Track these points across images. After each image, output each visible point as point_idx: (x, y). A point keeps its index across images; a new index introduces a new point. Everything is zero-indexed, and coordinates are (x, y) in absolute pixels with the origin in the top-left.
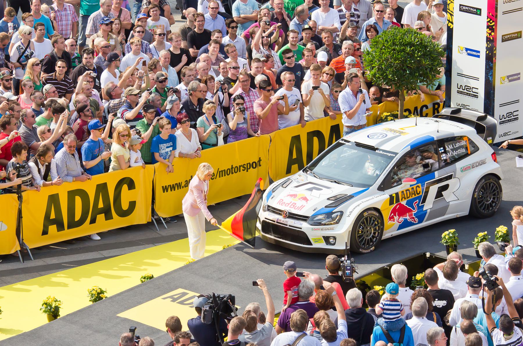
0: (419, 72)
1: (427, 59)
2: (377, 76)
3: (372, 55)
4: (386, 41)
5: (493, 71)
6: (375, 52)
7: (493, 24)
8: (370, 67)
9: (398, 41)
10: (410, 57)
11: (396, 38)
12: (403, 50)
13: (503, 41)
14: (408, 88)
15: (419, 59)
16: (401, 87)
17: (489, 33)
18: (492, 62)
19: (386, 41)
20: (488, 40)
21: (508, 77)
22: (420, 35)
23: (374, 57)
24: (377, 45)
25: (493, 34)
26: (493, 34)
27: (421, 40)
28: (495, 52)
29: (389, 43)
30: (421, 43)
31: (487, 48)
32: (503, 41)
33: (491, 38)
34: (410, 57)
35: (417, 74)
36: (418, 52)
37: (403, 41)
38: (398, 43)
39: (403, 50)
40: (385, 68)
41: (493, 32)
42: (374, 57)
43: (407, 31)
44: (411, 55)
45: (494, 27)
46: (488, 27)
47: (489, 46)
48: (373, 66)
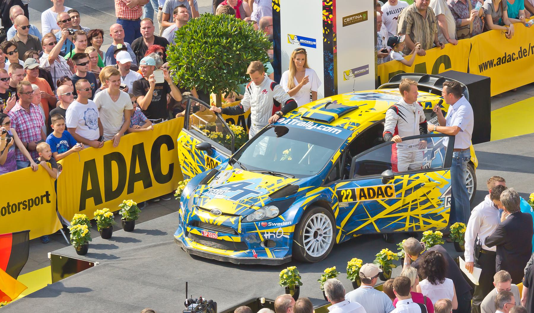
0: (239, 69)
1: (249, 53)
2: (186, 77)
3: (177, 52)
4: (196, 32)
5: (334, 64)
6: (182, 47)
7: (331, 3)
8: (176, 66)
9: (210, 31)
10: (228, 52)
11: (207, 27)
12: (218, 43)
13: (344, 25)
14: (226, 91)
15: (238, 52)
16: (218, 91)
17: (326, 16)
18: (332, 52)
19: (196, 32)
20: (325, 24)
21: (353, 71)
22: (238, 22)
23: (181, 54)
24: (183, 37)
25: (331, 16)
26: (331, 16)
27: (240, 29)
28: (335, 40)
29: (199, 35)
30: (240, 33)
31: (325, 35)
32: (344, 25)
33: (329, 22)
34: (228, 52)
35: (237, 73)
36: (237, 45)
37: (216, 31)
38: (210, 34)
39: (218, 43)
40: (196, 66)
41: (332, 14)
42: (181, 54)
43: (221, 19)
44: (228, 49)
45: (332, 8)
46: (325, 8)
47: (327, 33)
48: (180, 64)
